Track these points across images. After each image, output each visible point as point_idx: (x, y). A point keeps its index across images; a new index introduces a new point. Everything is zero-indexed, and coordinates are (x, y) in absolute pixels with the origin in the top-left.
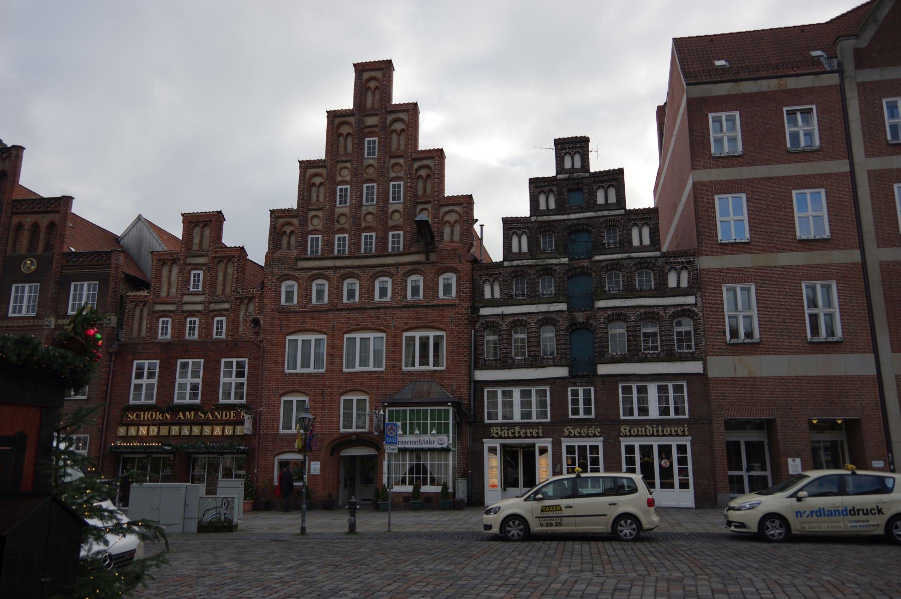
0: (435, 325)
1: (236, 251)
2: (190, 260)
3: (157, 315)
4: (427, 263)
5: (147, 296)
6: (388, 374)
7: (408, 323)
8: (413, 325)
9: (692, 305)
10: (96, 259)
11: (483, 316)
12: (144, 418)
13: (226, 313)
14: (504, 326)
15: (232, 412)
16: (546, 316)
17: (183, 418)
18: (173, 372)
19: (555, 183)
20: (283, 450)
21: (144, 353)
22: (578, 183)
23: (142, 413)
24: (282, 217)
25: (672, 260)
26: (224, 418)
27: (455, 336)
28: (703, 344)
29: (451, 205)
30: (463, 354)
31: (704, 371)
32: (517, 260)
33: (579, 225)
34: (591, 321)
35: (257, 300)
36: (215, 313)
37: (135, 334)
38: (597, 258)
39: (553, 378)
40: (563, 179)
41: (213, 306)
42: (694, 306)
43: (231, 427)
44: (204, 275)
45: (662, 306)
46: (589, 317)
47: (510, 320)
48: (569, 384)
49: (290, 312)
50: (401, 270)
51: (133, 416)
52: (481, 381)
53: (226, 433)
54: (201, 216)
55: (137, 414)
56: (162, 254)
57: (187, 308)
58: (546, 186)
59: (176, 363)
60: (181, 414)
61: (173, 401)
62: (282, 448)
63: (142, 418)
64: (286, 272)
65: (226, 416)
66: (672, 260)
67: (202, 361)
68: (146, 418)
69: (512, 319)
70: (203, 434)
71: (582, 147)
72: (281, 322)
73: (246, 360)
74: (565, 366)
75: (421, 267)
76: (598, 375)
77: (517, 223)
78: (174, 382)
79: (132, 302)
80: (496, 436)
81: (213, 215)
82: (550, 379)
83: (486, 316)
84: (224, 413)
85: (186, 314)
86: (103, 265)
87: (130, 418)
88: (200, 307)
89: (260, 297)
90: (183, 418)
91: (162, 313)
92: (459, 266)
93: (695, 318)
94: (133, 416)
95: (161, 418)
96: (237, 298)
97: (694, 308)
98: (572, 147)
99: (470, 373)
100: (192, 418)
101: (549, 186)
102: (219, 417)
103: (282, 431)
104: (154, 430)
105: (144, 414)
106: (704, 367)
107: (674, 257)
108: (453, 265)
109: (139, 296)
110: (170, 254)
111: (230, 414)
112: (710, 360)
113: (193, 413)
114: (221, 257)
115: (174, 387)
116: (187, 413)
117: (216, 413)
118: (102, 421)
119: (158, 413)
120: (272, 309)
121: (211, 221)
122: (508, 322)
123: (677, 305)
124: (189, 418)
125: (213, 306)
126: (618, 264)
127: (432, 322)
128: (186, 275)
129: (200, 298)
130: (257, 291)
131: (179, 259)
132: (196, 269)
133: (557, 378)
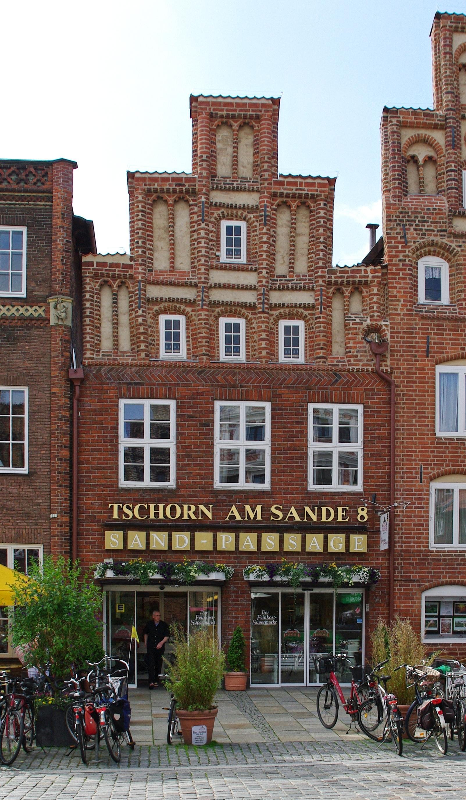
1: (320, 185)
2: (218, 197)
3: (156, 308)
5: (130, 267)
10: (14, 177)
12: (157, 514)
13: (306, 313)
15: (340, 509)
17: (238, 518)
18: (209, 425)
20: (440, 581)
21: (142, 384)
23: (152, 506)
24: (412, 126)
26: (324, 519)
35: (375, 291)
36: (282, 310)
37: (106, 344)
41: (276, 297)
43: (342, 537)
44: (248, 232)
49: (445, 319)
51: (132, 510)
53: (332, 548)
54: (238, 105)
55: (141, 508)
56: (156, 180)
57: (217, 296)
59: (213, 408)
60: (234, 508)
61: (212, 484)
62: (439, 577)
63: (152, 516)
64: (432, 238)
65: (328, 515)
67: (267, 405)
68: (161, 516)
70: (285, 550)
72: (428, 338)
73: (360, 408)
78: (212, 447)
79: (96, 276)
81: (263, 105)
84: (324, 509)
85: (218, 310)
86: (34, 192)
87: (127, 516)
88: (249, 297)
89: (379, 283)
90: (238, 518)
91: (166, 304)
94: (132, 510)
95: (193, 517)
96: (329, 283)
100: (259, 517)
102: (314, 518)
103: (433, 546)
104: (182, 541)
105: (157, 508)
109: (111, 265)
110: (174, 179)
111: (336, 511)
113: (259, 508)
114: (287, 196)
115: (212, 456)
116: (248, 508)
117: (307, 509)
118: (67, 519)
119: (186, 507)
120: (408, 310)
121: (258, 118)
124: (252, 516)
125: (276, 297)
128: (211, 228)
129: (250, 279)
130: (375, 271)
131: (194, 193)
132: (231, 217)
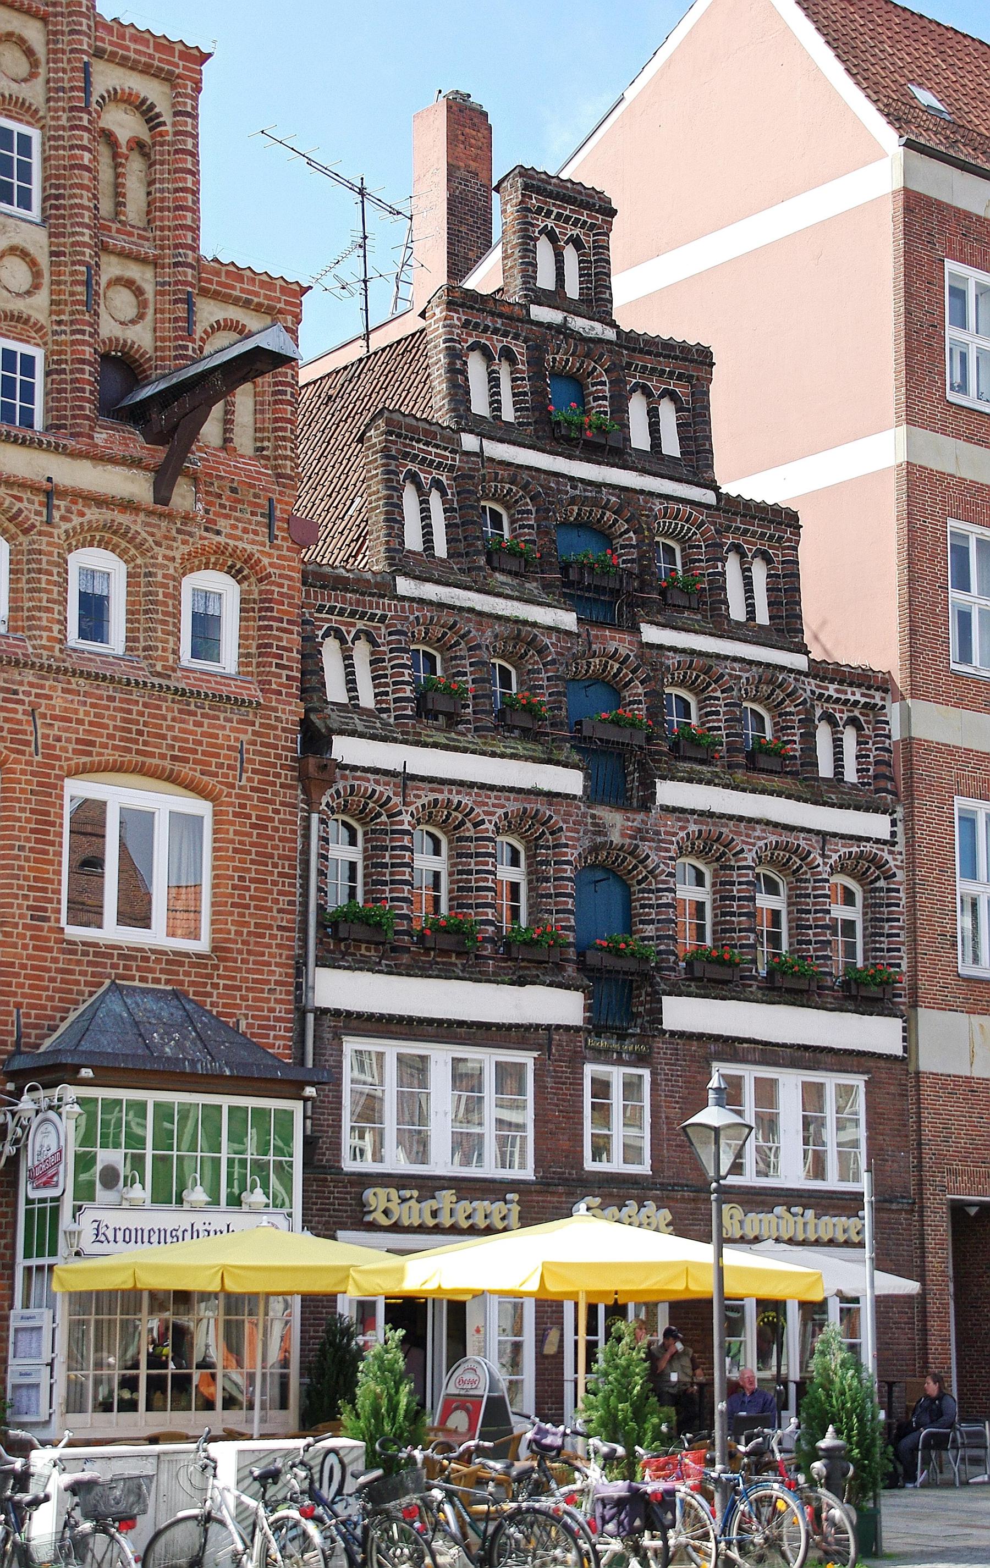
0: (186, 770)
4: (161, 515)
6: (14, 946)
7: (92, 744)
8: (111, 756)
9: (885, 842)
11: (346, 767)
14: (406, 818)
16: (528, 806)
19: (524, 330)
22: (588, 355)
25: (832, 690)
27: (253, 826)
28: (904, 968)
29: (236, 301)
30: (276, 901)
31: (905, 1049)
32: (438, 582)
33: (595, 502)
34: (645, 848)
38: (651, 634)
39: (548, 1027)
40: (549, 326)
42: (886, 848)
45: (818, 833)
46: (639, 830)
47: (425, 800)
48: (588, 1053)
50: (63, 518)
52: (337, 1013)
58: (496, 331)
66: (832, 690)
69: (432, 796)
71: (593, 226)
74: (577, 989)
75: (135, 523)
76: (664, 1032)
77: (427, 444)
80: (384, 1221)
82: (538, 1026)
83: (355, 768)
92: (270, 555)
93: (881, 883)
97: (886, 856)
98: (568, 218)
99: (299, 974)
101: (505, 335)
106: (905, 1039)
107: (841, 683)
108: (248, 547)
112: (927, 1018)
122: (419, 803)
123: (851, 837)
126: (707, 671)
127: (174, 758)
133: (558, 1027)
